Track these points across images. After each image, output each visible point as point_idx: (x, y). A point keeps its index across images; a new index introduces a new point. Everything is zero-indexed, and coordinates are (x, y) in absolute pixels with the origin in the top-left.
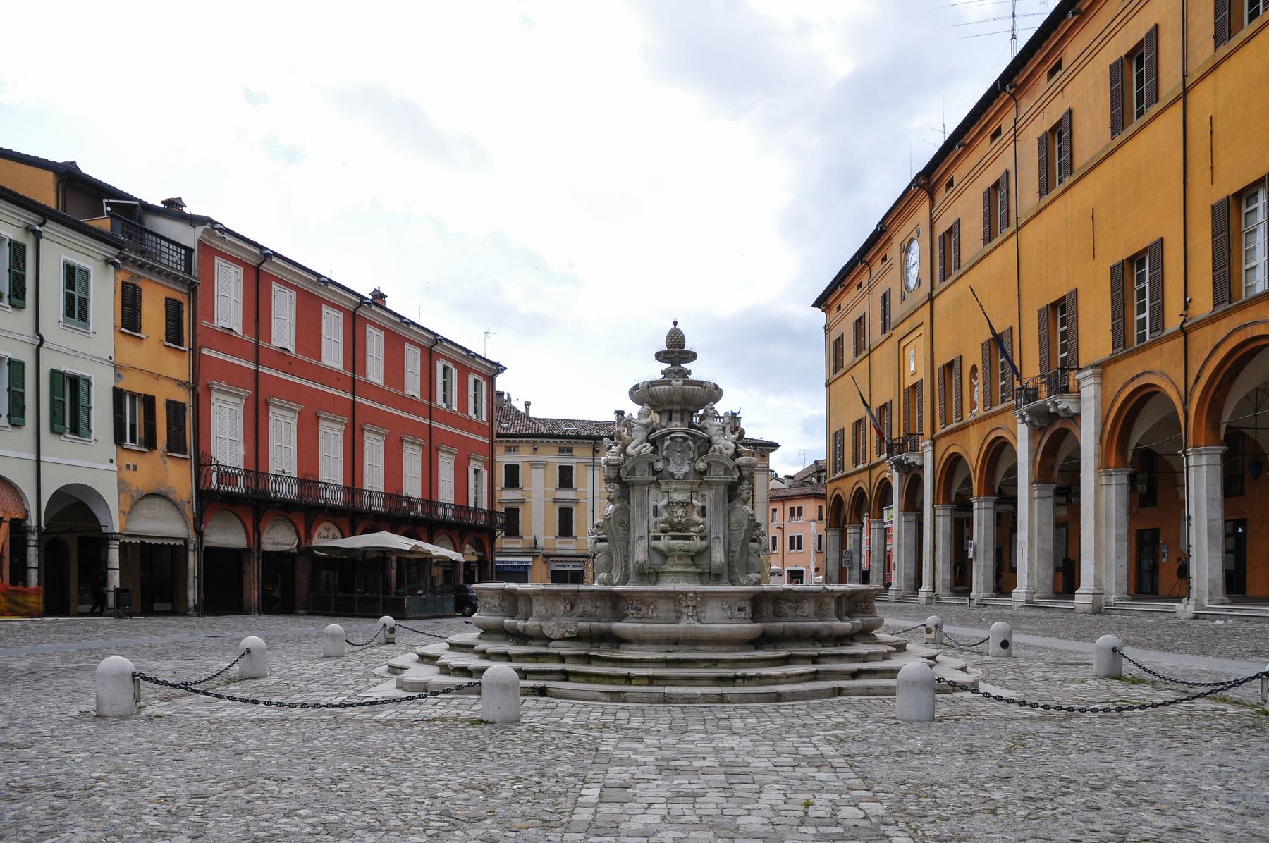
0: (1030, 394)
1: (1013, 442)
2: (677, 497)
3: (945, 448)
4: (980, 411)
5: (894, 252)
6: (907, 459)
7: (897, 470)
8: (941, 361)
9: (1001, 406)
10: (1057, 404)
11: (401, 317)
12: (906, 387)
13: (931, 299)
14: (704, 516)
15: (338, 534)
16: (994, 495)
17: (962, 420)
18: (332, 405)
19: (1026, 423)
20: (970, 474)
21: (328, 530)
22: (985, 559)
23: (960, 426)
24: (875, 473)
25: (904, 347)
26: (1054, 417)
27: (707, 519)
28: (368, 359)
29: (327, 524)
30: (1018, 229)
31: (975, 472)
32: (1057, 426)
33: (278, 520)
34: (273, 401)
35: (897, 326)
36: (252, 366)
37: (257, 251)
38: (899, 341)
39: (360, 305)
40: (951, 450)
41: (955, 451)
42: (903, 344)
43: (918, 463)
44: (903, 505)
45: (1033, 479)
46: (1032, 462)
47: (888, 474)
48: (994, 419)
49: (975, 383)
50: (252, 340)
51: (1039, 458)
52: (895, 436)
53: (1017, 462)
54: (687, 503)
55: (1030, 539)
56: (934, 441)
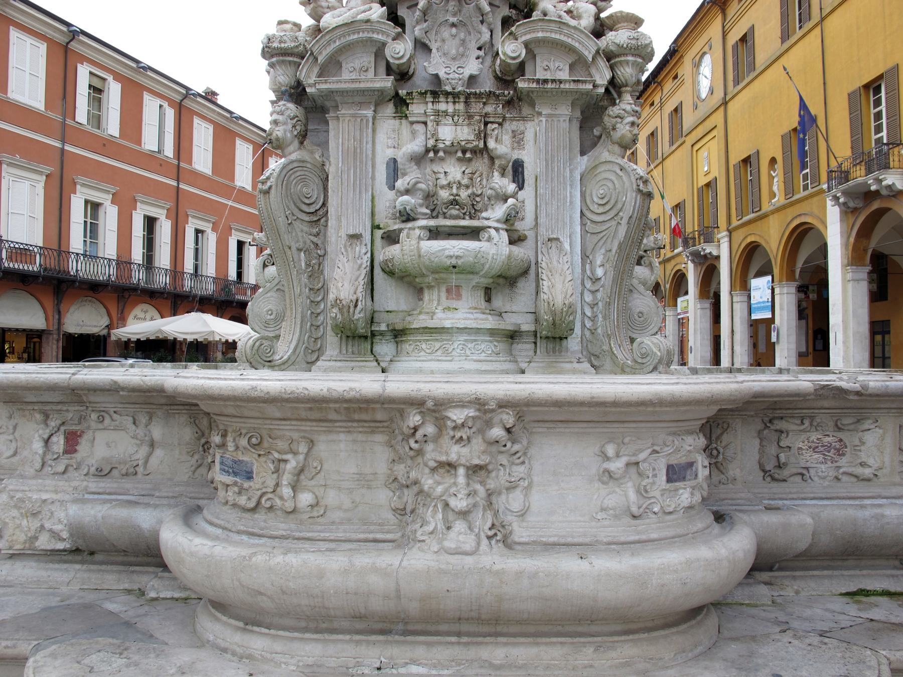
0: (845, 176)
1: (820, 226)
2: (448, 133)
3: (741, 238)
4: (779, 199)
5: (685, 69)
6: (704, 250)
7: (693, 261)
8: (736, 157)
9: (802, 194)
10: (881, 181)
11: (231, 112)
12: (700, 185)
13: (725, 103)
14: (520, 183)
15: (156, 314)
16: (794, 280)
17: (760, 210)
18: (154, 191)
19: (839, 204)
20: (770, 261)
21: (146, 312)
22: (788, 343)
23: (758, 216)
24: (669, 266)
25: (697, 151)
26: (869, 196)
27: (527, 193)
28: (195, 149)
29: (145, 306)
30: (823, 19)
31: (776, 259)
32: (876, 205)
33: (86, 301)
34: (80, 179)
35: (690, 133)
36: (58, 144)
37: (64, 29)
38: (692, 146)
39: (186, 97)
40: (749, 240)
41: (753, 240)
42: (696, 147)
43: (715, 253)
44: (697, 292)
45: (846, 261)
46: (845, 245)
47: (683, 266)
48: (798, 206)
49: (774, 175)
50: (59, 118)
51: (852, 240)
52: (689, 229)
53: (825, 245)
54: (474, 151)
55: (845, 321)
56: (730, 232)
